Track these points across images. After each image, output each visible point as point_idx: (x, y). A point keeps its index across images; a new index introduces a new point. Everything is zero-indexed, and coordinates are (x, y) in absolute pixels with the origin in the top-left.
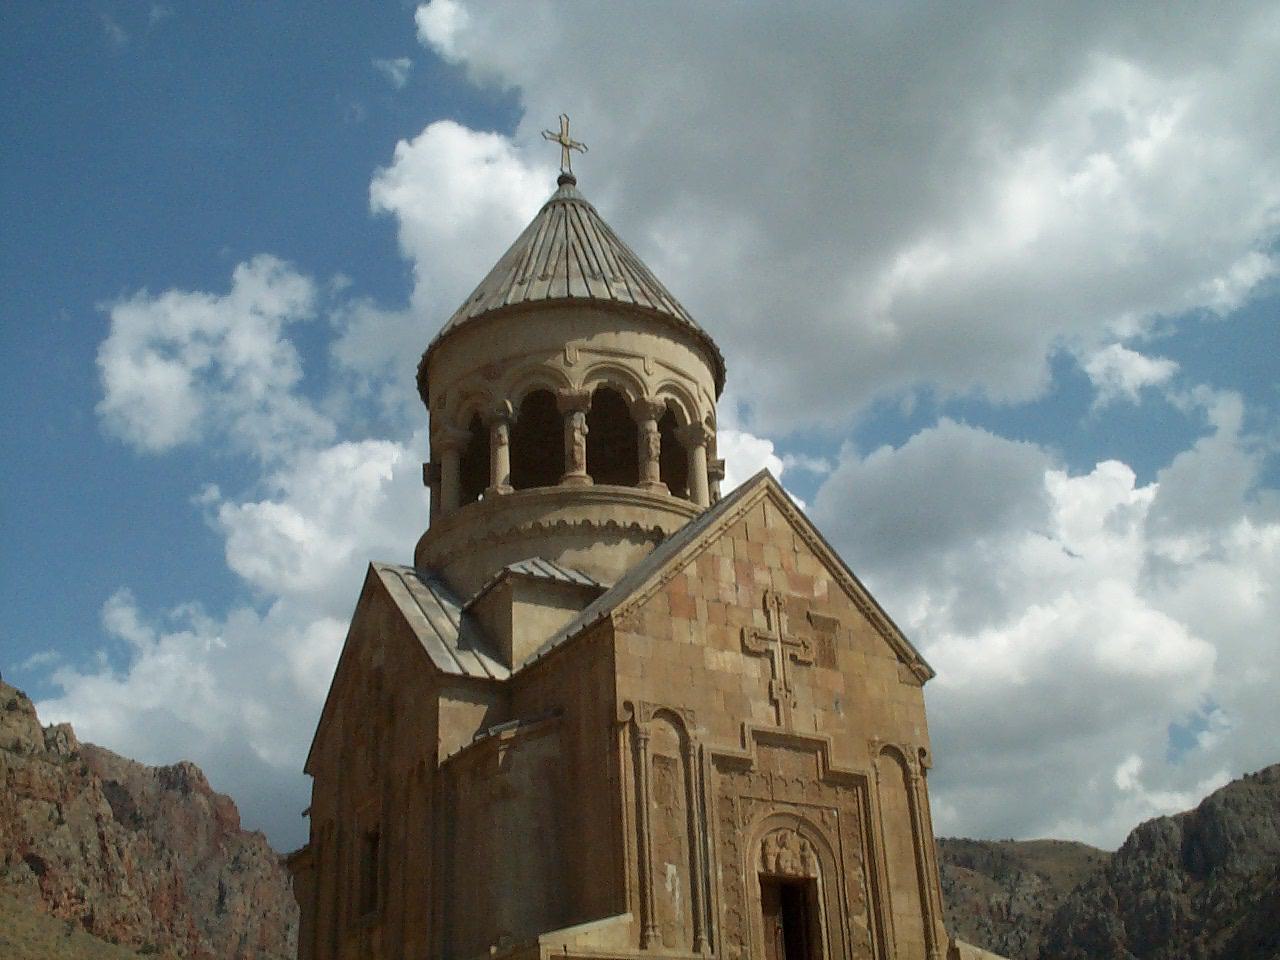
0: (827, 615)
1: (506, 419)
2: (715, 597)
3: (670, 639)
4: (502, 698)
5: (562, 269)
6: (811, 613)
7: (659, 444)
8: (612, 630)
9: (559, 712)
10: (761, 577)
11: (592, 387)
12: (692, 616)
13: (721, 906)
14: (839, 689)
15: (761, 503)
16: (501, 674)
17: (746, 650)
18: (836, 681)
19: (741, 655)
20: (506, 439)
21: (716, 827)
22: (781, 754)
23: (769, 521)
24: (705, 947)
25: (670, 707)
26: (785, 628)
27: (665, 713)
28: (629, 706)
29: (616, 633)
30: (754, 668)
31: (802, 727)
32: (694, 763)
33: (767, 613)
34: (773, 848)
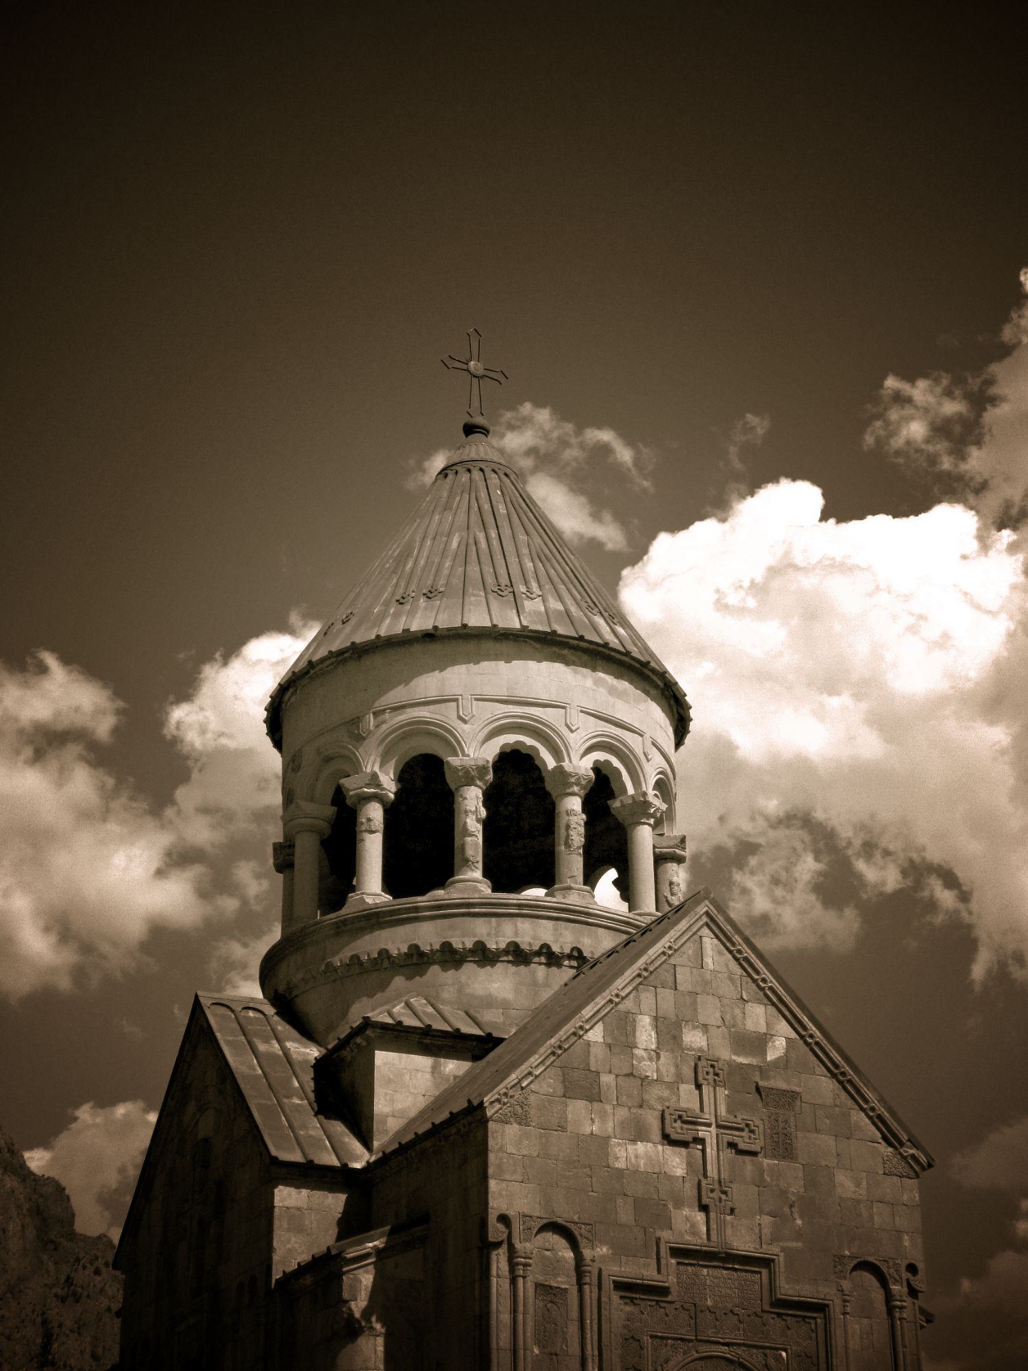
2: (626, 1070)
3: (564, 1129)
6: (761, 1083)
7: (582, 830)
8: (484, 1121)
9: (425, 1219)
10: (694, 1039)
12: (593, 1095)
14: (796, 1187)
15: (696, 937)
17: (667, 1139)
19: (660, 1147)
23: (709, 961)
25: (560, 1221)
26: (722, 1110)
28: (504, 1219)
29: (491, 1124)
30: (676, 1163)
31: (742, 1242)
32: (590, 1293)
33: (699, 1087)
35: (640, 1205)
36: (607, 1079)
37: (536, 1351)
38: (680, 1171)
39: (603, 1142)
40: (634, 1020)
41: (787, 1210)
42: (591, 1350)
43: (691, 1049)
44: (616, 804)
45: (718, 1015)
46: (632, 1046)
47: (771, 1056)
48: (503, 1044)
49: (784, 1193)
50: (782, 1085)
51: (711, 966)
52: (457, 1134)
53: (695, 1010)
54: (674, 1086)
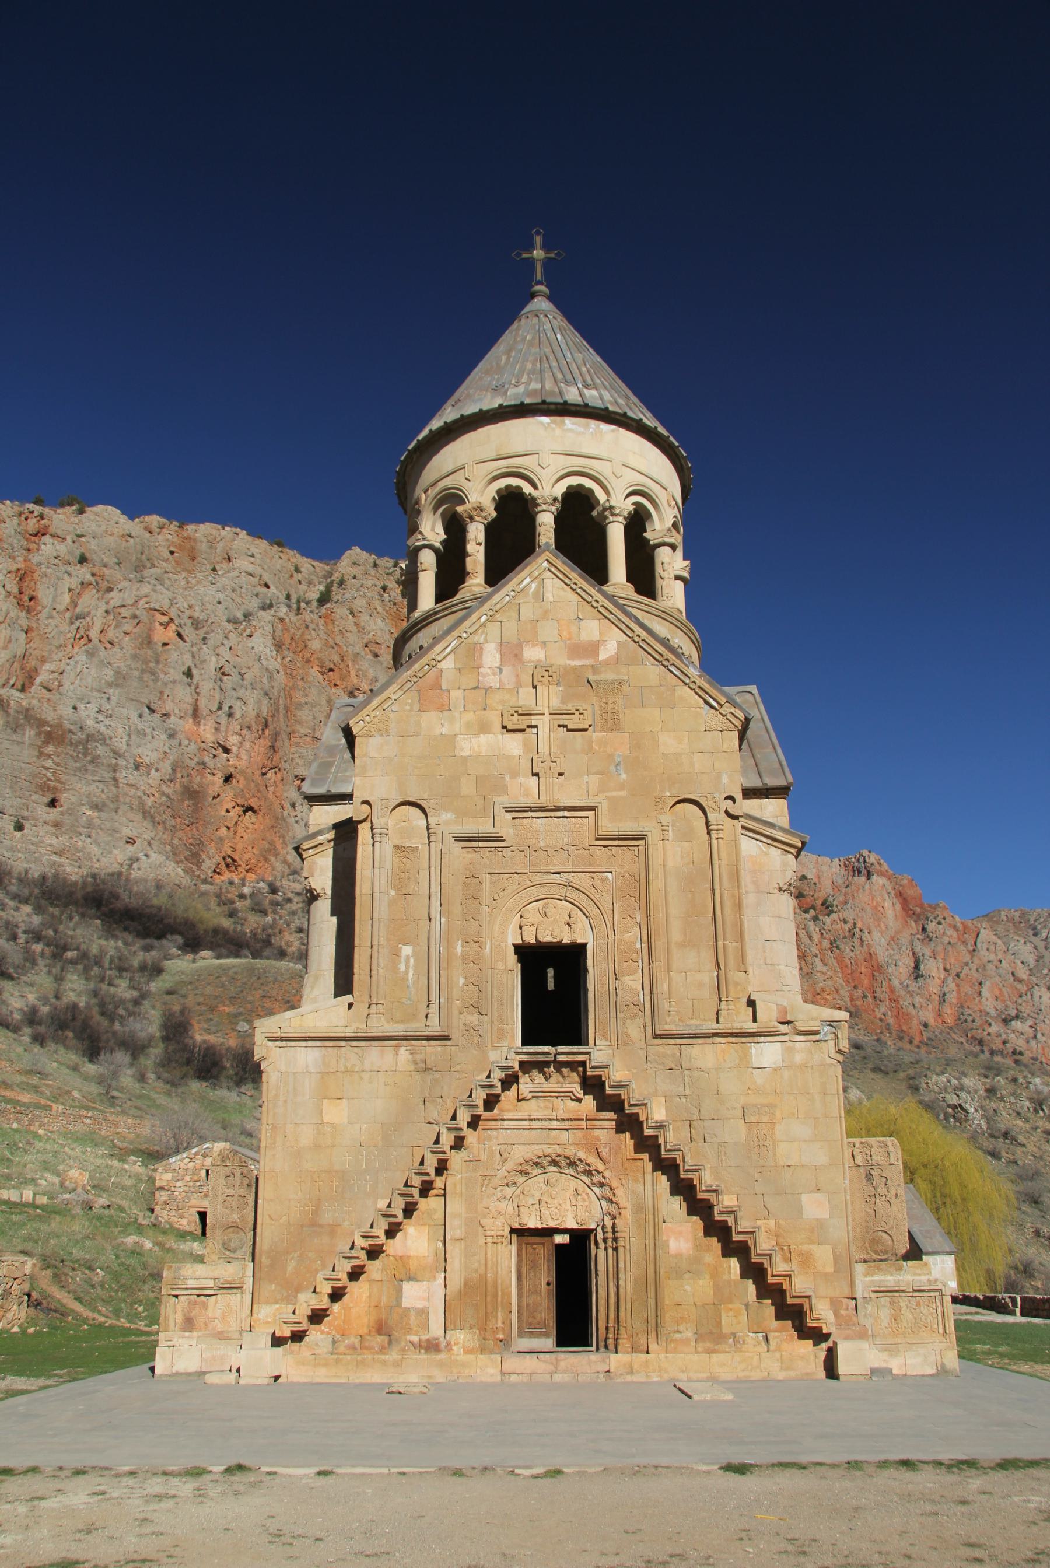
0: (613, 677)
1: (430, 547)
10: (533, 654)
12: (443, 708)
18: (620, 745)
19: (500, 736)
22: (541, 824)
23: (549, 596)
24: (434, 1020)
30: (513, 744)
33: (535, 687)
35: (480, 780)
36: (456, 694)
37: (393, 893)
39: (450, 740)
40: (482, 648)
41: (612, 768)
43: (530, 661)
44: (595, 513)
45: (556, 633)
47: (603, 656)
49: (610, 756)
50: (611, 676)
51: (551, 599)
53: (536, 632)
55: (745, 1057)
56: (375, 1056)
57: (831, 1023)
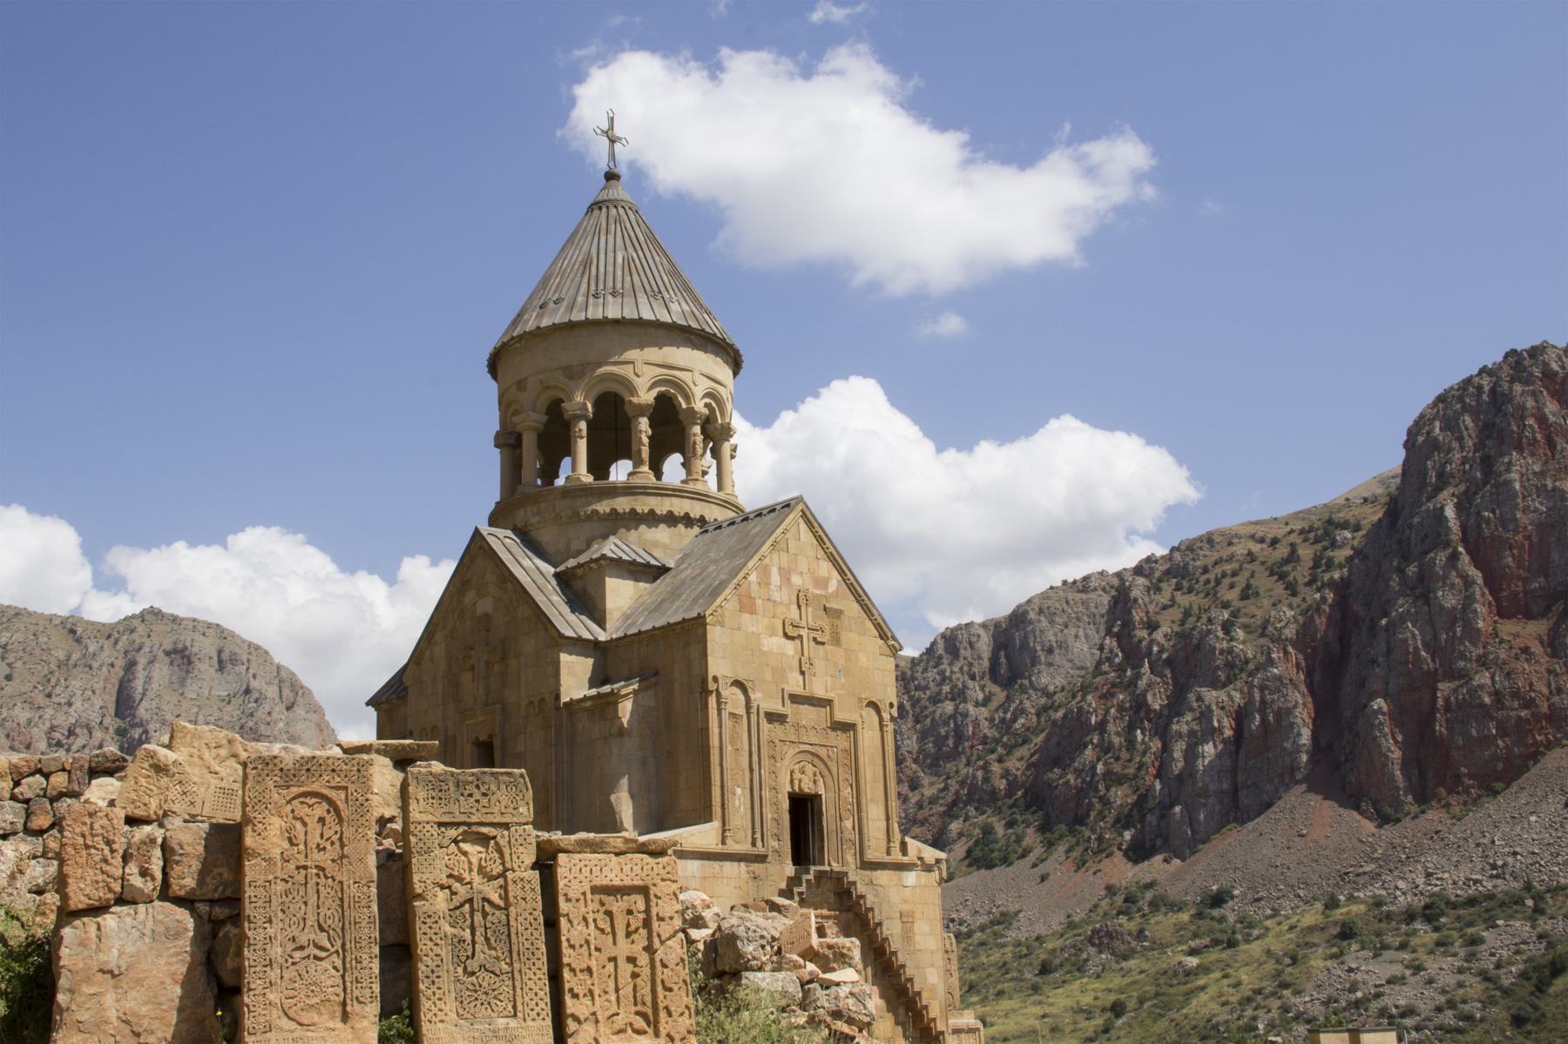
4: (609, 660)
5: (628, 285)
8: (704, 625)
9: (656, 674)
10: (796, 580)
11: (654, 393)
12: (753, 612)
13: (768, 815)
16: (602, 637)
17: (786, 636)
18: (838, 654)
20: (584, 433)
21: (766, 762)
22: (805, 709)
24: (759, 844)
27: (738, 684)
28: (715, 679)
30: (790, 648)
31: (819, 692)
32: (754, 718)
34: (797, 775)
36: (759, 602)
38: (791, 652)
42: (754, 749)
46: (768, 584)
48: (672, 573)
52: (692, 632)
54: (788, 606)
55: (900, 878)
56: (730, 868)
57: (938, 861)
